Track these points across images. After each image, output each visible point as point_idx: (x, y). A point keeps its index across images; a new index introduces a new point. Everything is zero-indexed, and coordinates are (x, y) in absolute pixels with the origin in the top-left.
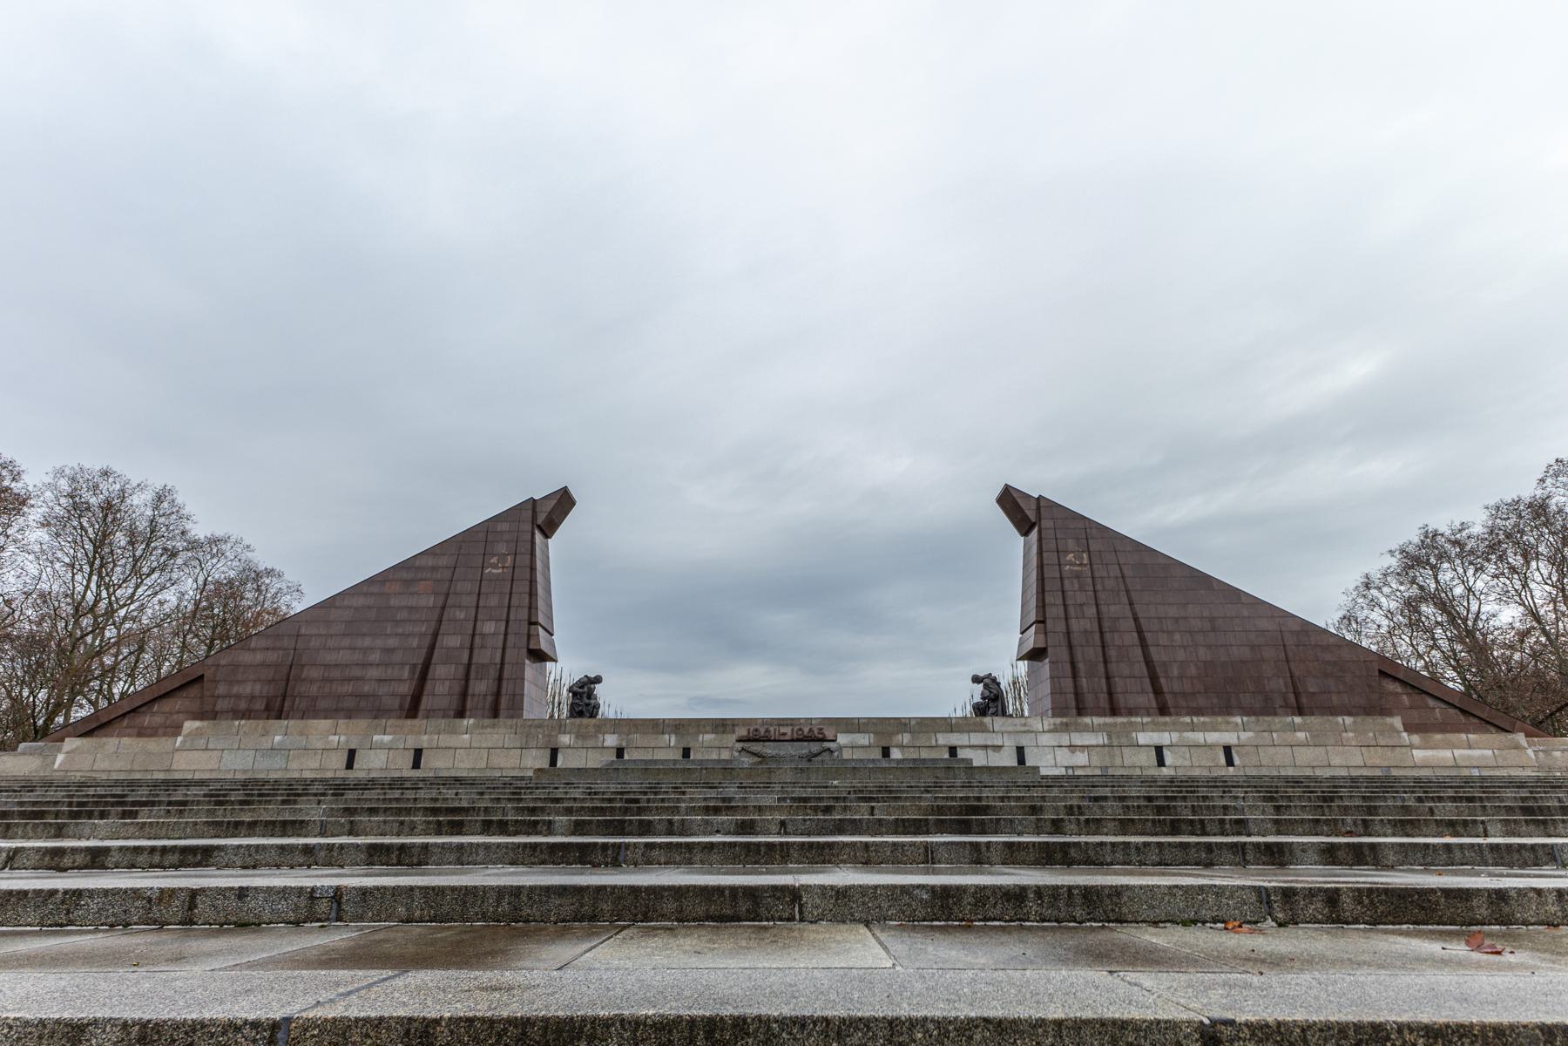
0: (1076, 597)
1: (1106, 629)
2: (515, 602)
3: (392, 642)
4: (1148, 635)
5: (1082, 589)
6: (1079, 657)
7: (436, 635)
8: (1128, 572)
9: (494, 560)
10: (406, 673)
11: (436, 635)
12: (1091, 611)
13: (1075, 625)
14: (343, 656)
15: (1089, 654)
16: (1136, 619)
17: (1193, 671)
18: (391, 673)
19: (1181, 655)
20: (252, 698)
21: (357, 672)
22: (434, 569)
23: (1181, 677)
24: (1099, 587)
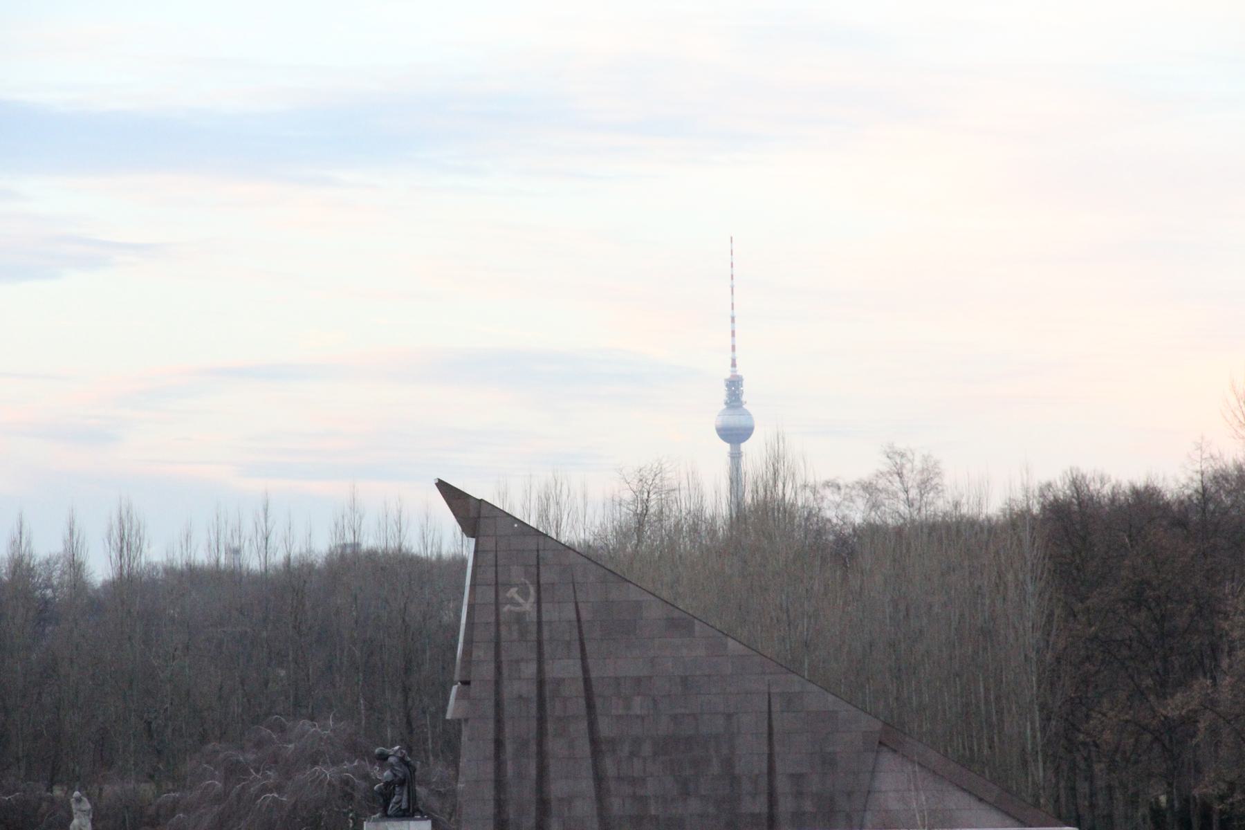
1: (547, 694)
4: (599, 703)
6: (508, 730)
8: (585, 615)
12: (530, 670)
13: (511, 689)
15: (520, 725)
16: (587, 681)
17: (647, 749)
23: (632, 754)
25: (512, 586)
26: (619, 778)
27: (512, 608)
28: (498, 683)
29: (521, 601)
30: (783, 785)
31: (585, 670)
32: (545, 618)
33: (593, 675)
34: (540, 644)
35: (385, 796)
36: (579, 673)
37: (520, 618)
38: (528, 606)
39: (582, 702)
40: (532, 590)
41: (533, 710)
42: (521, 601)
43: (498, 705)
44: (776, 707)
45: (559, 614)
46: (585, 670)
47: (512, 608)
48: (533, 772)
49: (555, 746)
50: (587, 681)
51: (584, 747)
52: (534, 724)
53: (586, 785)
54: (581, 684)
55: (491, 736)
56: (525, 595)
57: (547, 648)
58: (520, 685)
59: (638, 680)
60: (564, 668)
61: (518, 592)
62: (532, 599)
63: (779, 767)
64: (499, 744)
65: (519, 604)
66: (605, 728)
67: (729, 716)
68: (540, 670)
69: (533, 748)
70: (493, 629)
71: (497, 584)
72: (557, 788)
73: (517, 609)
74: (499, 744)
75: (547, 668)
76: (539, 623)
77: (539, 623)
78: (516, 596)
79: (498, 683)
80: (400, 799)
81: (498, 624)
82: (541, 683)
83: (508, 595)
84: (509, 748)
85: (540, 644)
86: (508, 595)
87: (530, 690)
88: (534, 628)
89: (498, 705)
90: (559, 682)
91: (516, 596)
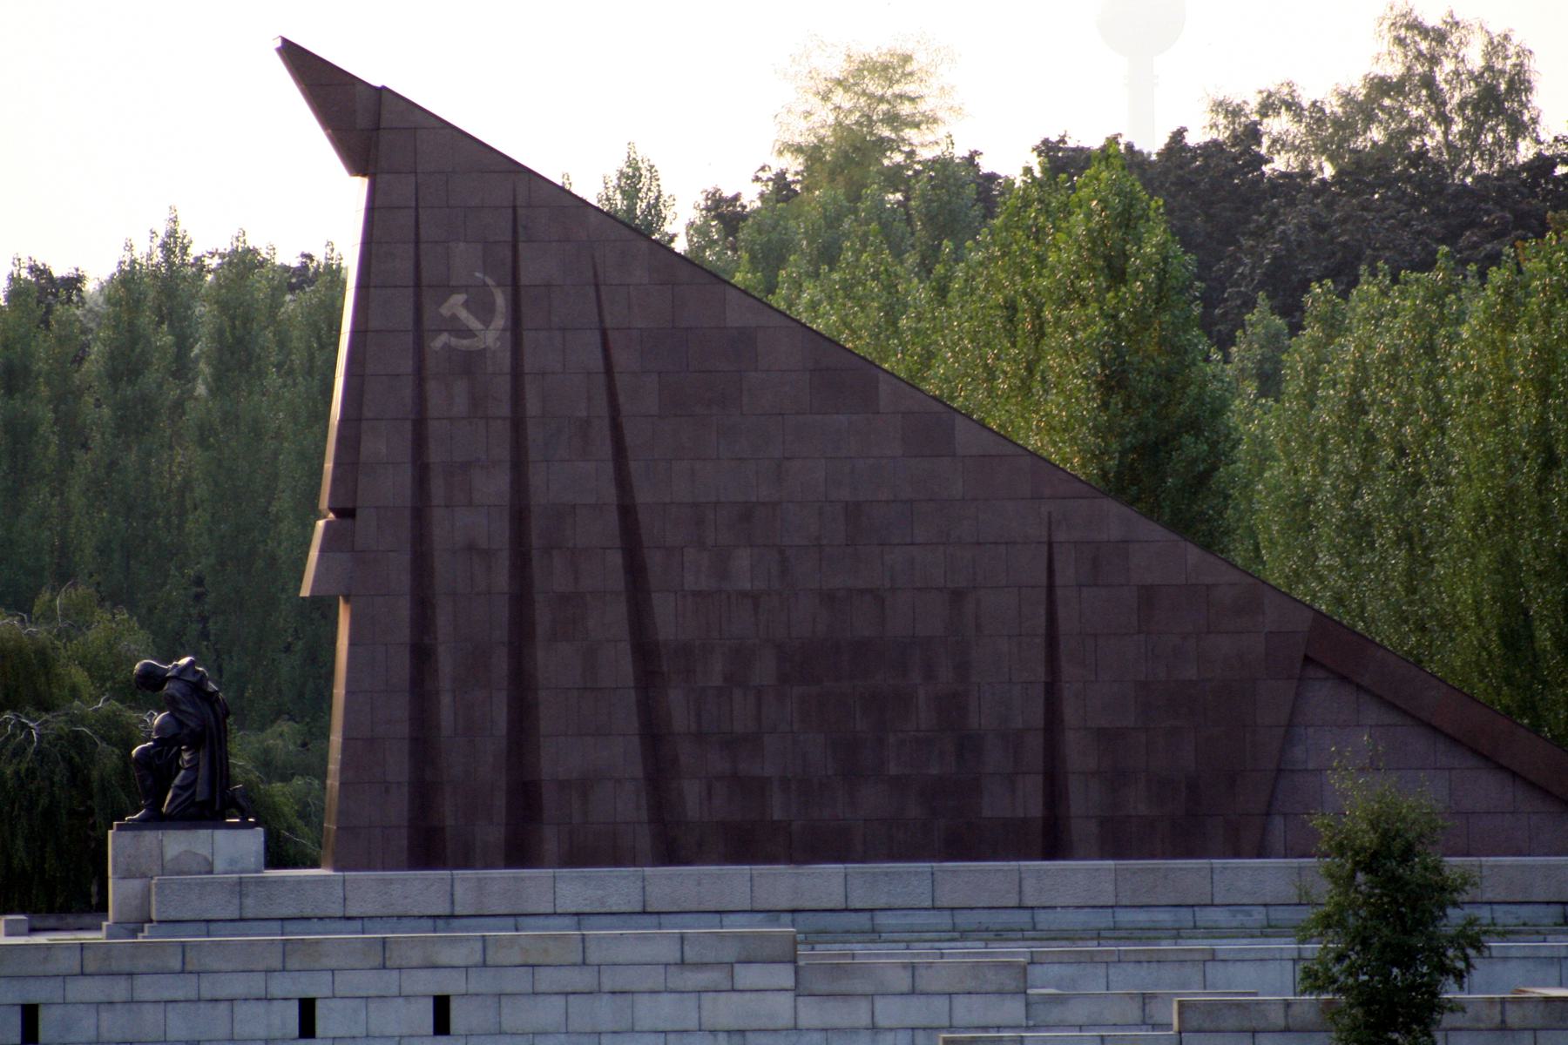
1: (535, 540)
4: (654, 561)
12: (494, 486)
13: (448, 528)
16: (627, 513)
24: (532, 406)
25: (455, 290)
27: (454, 341)
28: (420, 514)
29: (475, 324)
30: (1079, 755)
31: (623, 482)
32: (529, 364)
33: (643, 495)
34: (518, 424)
35: (158, 767)
36: (610, 494)
37: (469, 364)
38: (491, 336)
39: (616, 559)
40: (501, 300)
41: (501, 579)
42: (475, 324)
44: (1067, 574)
46: (623, 482)
47: (454, 341)
48: (500, 713)
49: (553, 663)
50: (627, 513)
51: (620, 666)
52: (502, 611)
53: (621, 753)
54: (613, 517)
55: (405, 634)
56: (484, 310)
57: (534, 434)
58: (473, 519)
60: (573, 480)
61: (466, 304)
62: (500, 321)
63: (1071, 714)
64: (422, 655)
65: (469, 333)
66: (670, 620)
67: (957, 596)
69: (501, 664)
70: (408, 392)
71: (417, 285)
72: (559, 758)
73: (465, 343)
74: (422, 655)
75: (537, 477)
76: (517, 374)
77: (517, 374)
78: (463, 314)
79: (420, 514)
82: (520, 515)
83: (445, 310)
84: (446, 661)
85: (518, 424)
86: (445, 310)
87: (497, 533)
88: (503, 385)
91: (463, 314)
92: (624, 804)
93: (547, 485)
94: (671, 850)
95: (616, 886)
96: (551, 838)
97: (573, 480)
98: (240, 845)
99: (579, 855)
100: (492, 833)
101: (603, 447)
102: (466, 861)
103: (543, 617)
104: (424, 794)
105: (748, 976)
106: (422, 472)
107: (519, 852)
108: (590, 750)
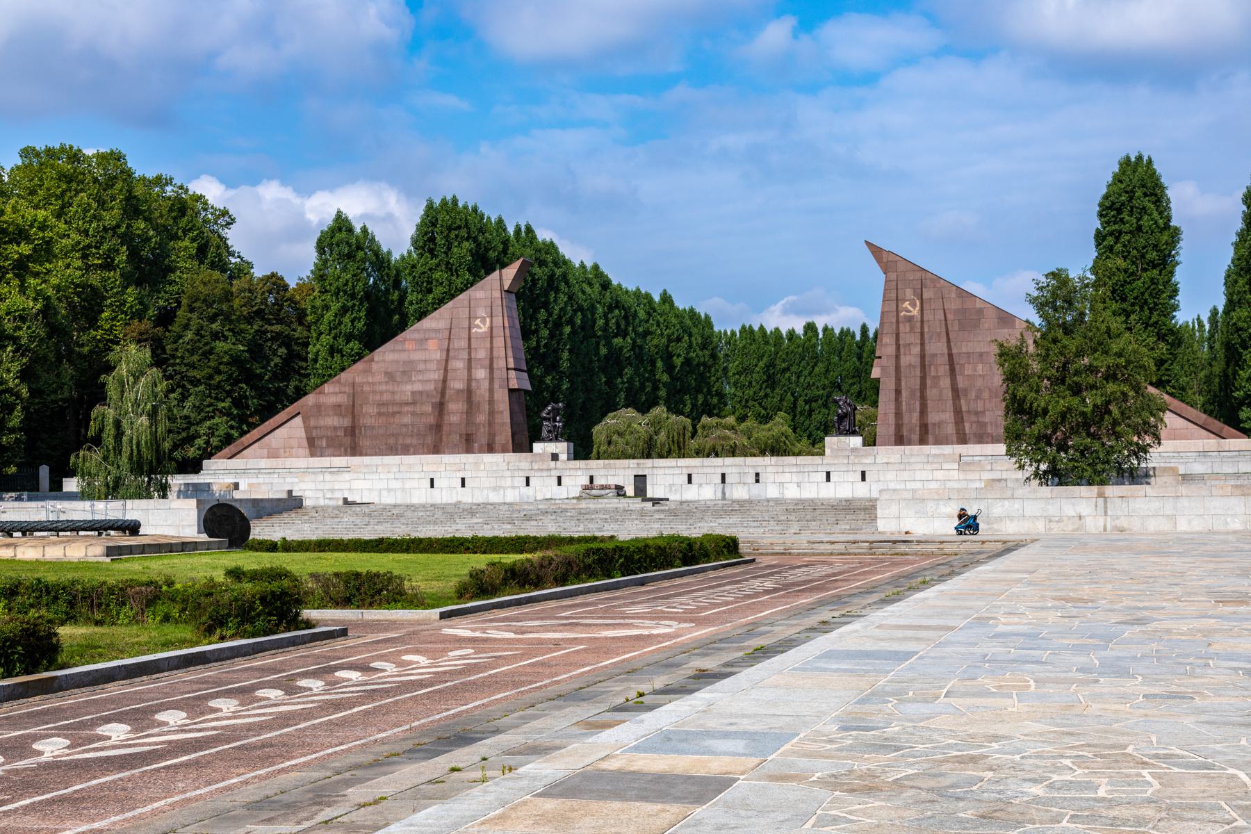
0: (906, 338)
2: (495, 353)
3: (418, 387)
4: (957, 367)
5: (912, 329)
7: (445, 381)
9: (478, 322)
10: (429, 409)
11: (445, 381)
12: (916, 350)
13: (904, 361)
14: (386, 397)
15: (911, 381)
16: (950, 355)
18: (418, 409)
19: (979, 383)
20: (335, 428)
21: (396, 409)
22: (436, 331)
24: (926, 329)
26: (969, 412)
28: (897, 357)
31: (949, 348)
32: (925, 319)
33: (954, 351)
34: (922, 334)
36: (946, 351)
38: (915, 312)
43: (898, 368)
45: (934, 318)
46: (949, 348)
49: (931, 393)
50: (950, 355)
52: (918, 382)
53: (948, 416)
56: (914, 306)
57: (926, 336)
58: (910, 358)
59: (981, 354)
68: (923, 350)
72: (932, 418)
75: (927, 348)
76: (922, 321)
77: (922, 321)
79: (897, 357)
80: (846, 424)
81: (898, 322)
82: (923, 357)
84: (904, 394)
85: (922, 334)
87: (916, 361)
88: (918, 325)
89: (898, 368)
90: (934, 355)
92: (950, 429)
93: (931, 348)
94: (963, 439)
95: (947, 449)
96: (931, 438)
97: (937, 347)
98: (856, 441)
99: (938, 442)
100: (916, 437)
101: (944, 339)
102: (909, 444)
103: (929, 382)
104: (898, 427)
105: (946, 466)
106: (898, 347)
107: (923, 441)
108: (942, 415)
